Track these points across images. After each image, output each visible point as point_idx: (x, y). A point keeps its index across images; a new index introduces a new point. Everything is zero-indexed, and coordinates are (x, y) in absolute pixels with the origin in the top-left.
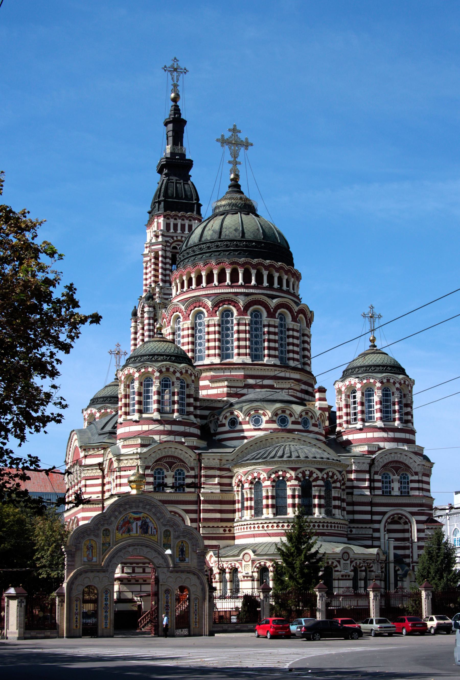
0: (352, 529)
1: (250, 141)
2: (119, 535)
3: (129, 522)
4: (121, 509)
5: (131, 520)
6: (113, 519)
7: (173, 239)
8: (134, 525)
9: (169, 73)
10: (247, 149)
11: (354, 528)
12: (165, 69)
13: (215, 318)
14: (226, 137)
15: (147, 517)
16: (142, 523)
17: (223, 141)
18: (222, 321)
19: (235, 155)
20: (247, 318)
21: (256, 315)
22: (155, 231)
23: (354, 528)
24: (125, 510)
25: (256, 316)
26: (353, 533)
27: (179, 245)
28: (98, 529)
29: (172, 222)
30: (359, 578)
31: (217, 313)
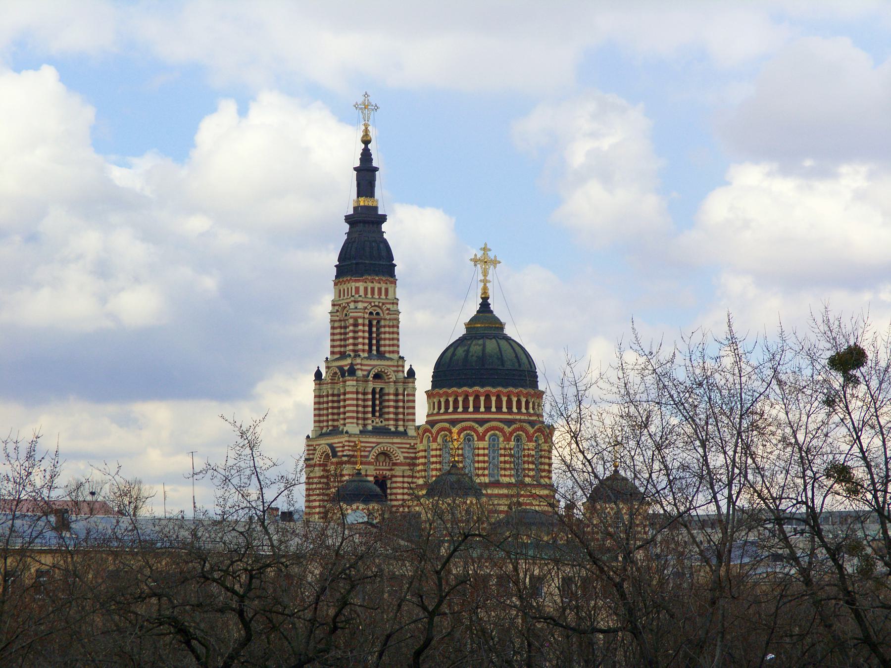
1: (498, 259)
7: (371, 305)
9: (360, 111)
10: (495, 267)
12: (356, 106)
13: (484, 442)
14: (478, 256)
17: (475, 261)
18: (489, 444)
19: (485, 274)
20: (512, 444)
21: (518, 439)
22: (353, 296)
25: (518, 440)
27: (375, 310)
29: (370, 285)
31: (487, 438)
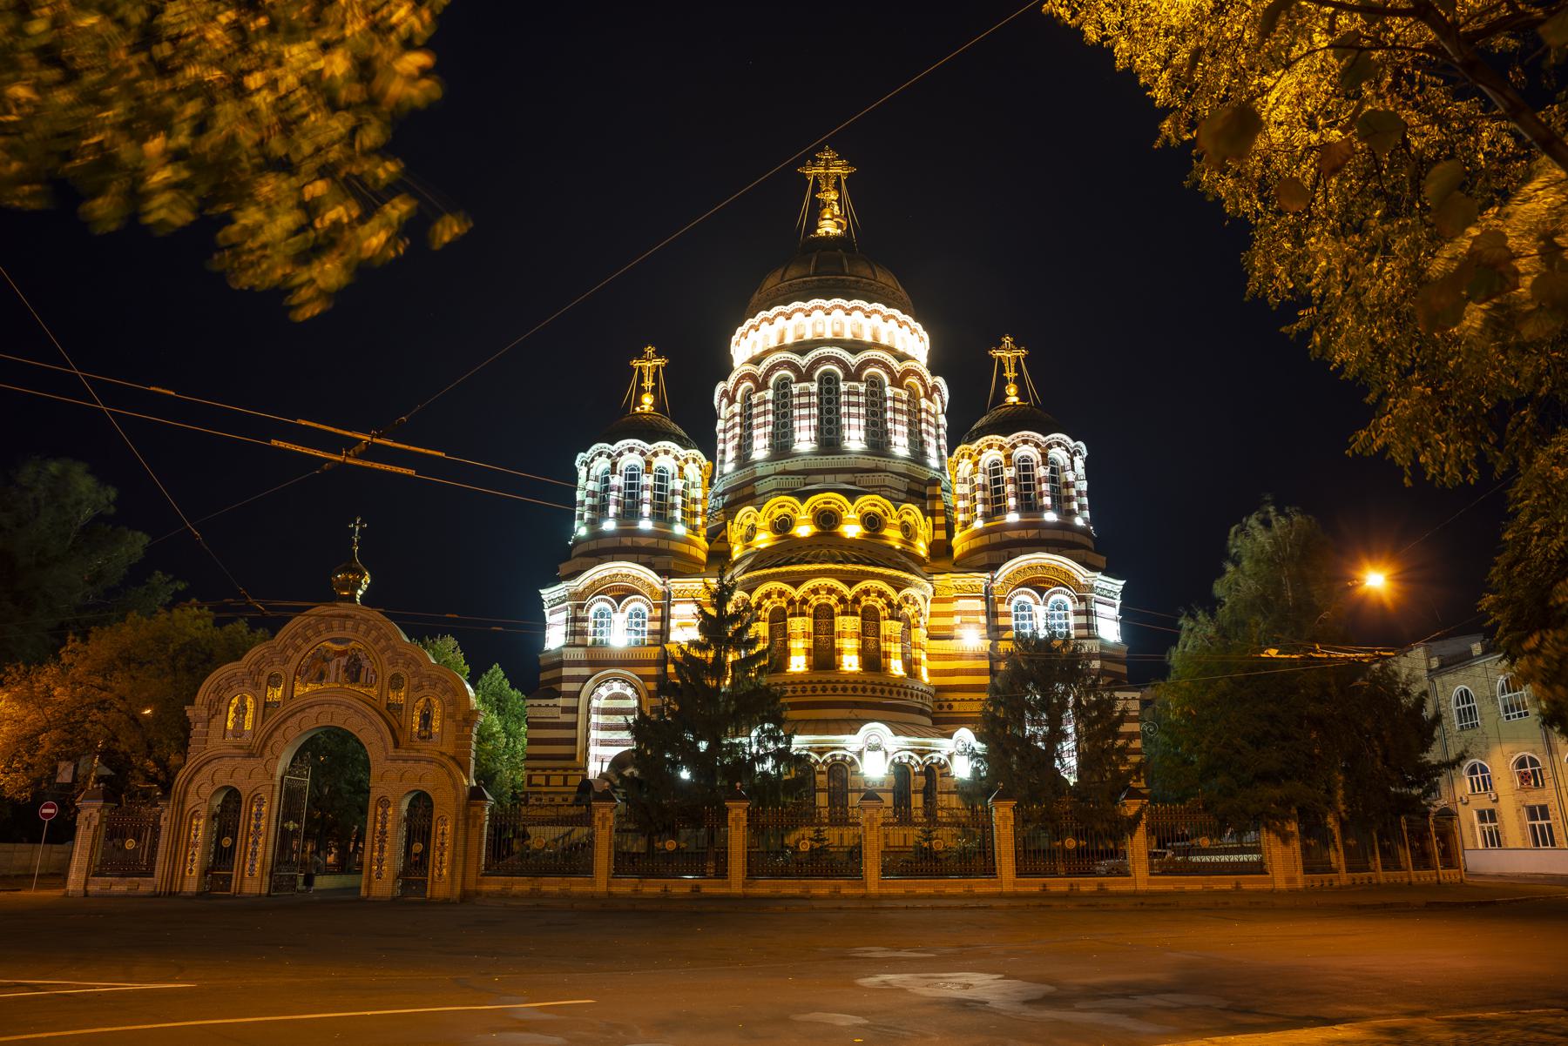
0: (953, 703)
2: (301, 690)
3: (325, 660)
4: (309, 633)
5: (328, 656)
6: (290, 652)
8: (333, 665)
11: (955, 700)
15: (360, 650)
16: (349, 660)
21: (828, 380)
23: (955, 700)
24: (318, 633)
26: (954, 710)
28: (260, 672)
30: (913, 789)
